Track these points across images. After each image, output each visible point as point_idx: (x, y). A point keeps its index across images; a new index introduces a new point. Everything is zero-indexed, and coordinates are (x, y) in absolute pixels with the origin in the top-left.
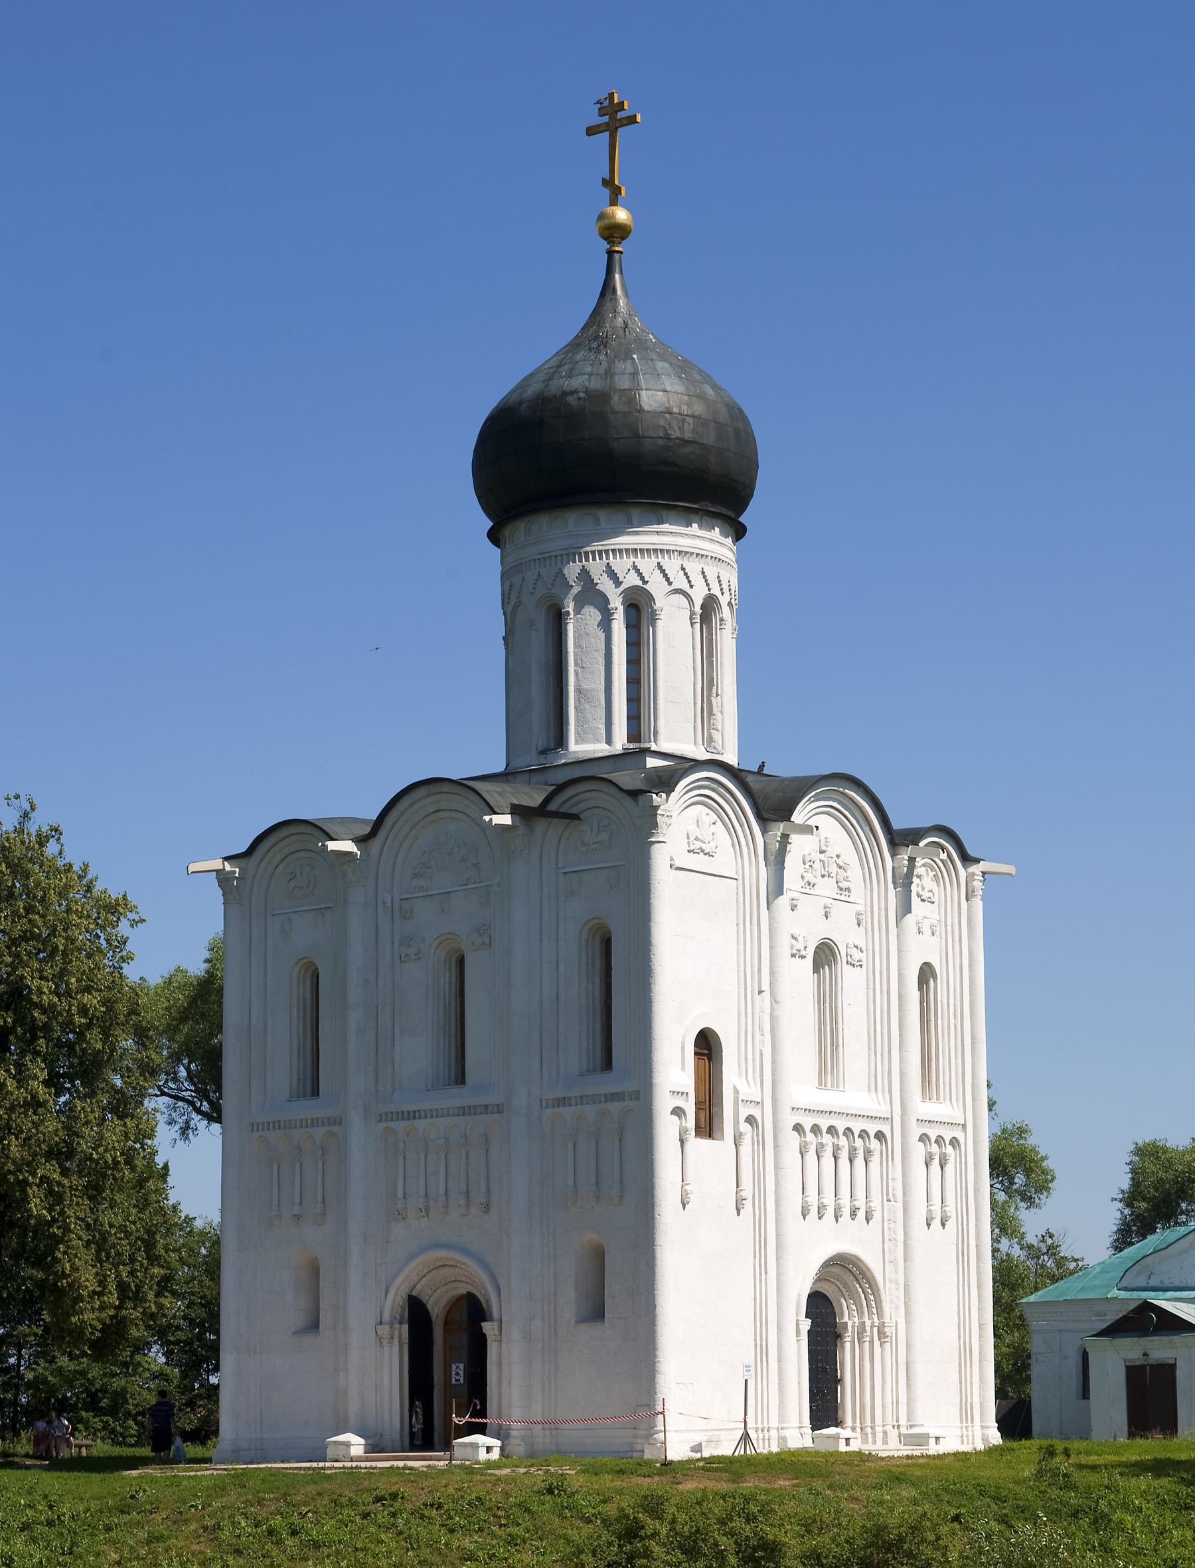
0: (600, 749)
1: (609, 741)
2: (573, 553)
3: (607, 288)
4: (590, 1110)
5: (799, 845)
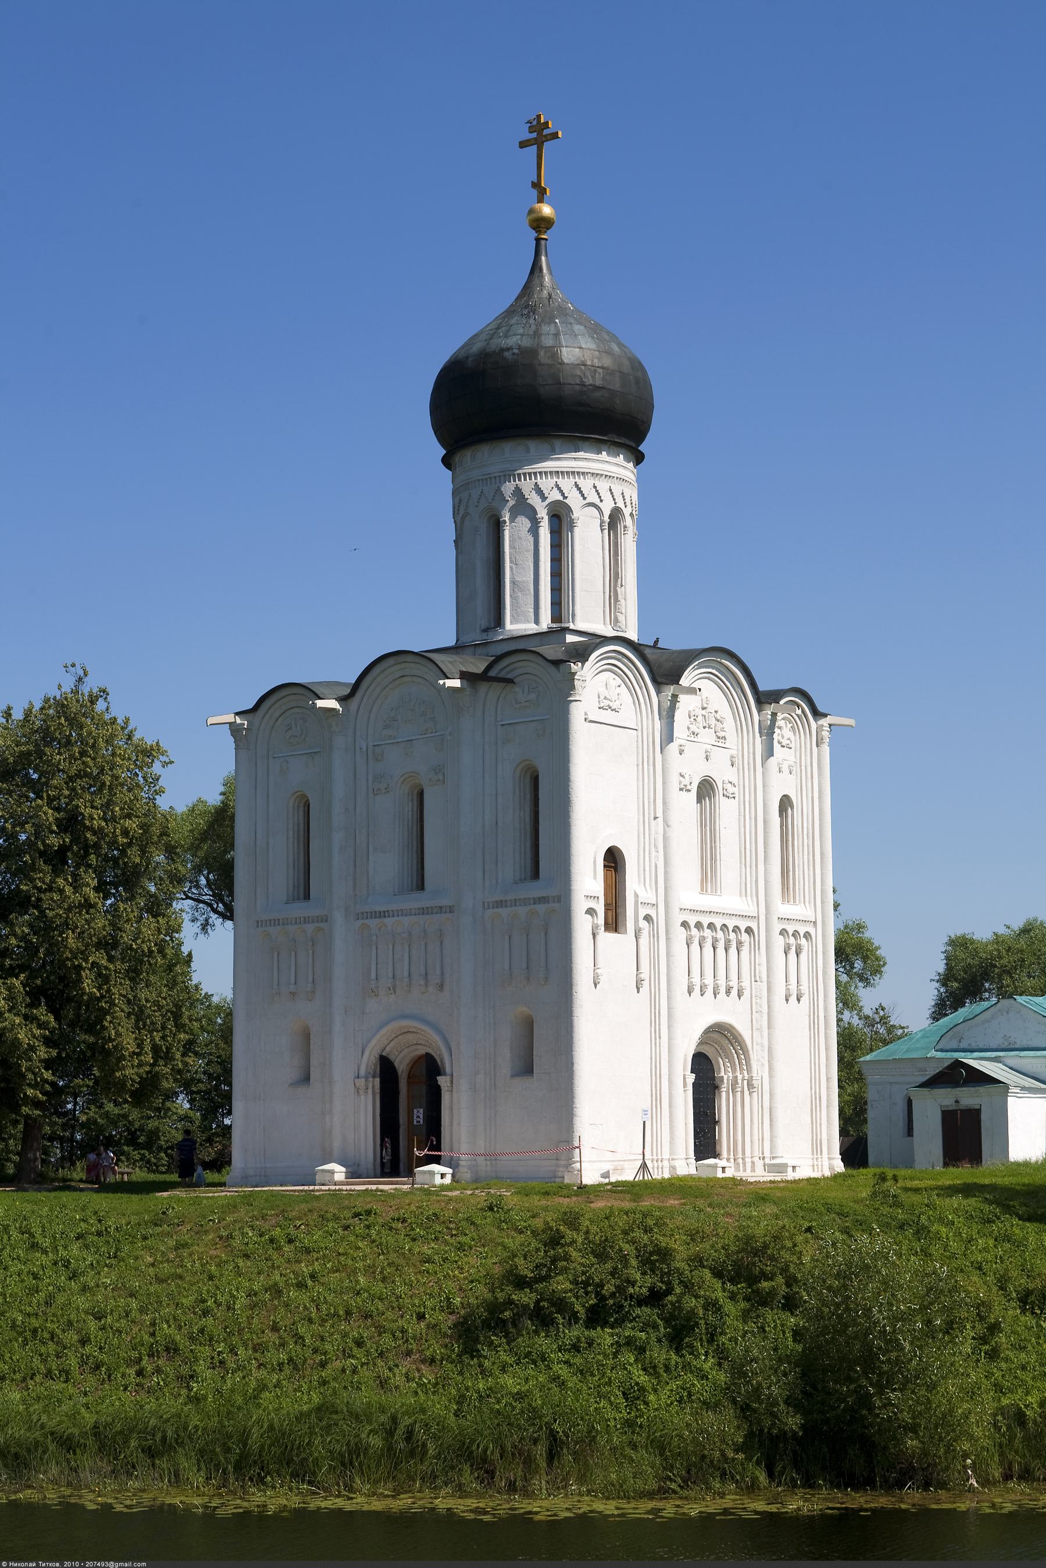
0: (531, 628)
1: (537, 621)
2: (508, 475)
3: (536, 268)
4: (522, 911)
5: (686, 704)
